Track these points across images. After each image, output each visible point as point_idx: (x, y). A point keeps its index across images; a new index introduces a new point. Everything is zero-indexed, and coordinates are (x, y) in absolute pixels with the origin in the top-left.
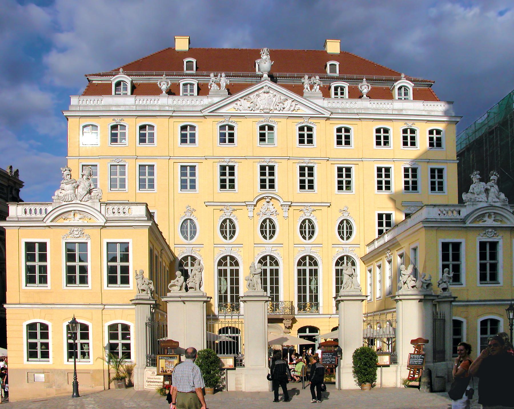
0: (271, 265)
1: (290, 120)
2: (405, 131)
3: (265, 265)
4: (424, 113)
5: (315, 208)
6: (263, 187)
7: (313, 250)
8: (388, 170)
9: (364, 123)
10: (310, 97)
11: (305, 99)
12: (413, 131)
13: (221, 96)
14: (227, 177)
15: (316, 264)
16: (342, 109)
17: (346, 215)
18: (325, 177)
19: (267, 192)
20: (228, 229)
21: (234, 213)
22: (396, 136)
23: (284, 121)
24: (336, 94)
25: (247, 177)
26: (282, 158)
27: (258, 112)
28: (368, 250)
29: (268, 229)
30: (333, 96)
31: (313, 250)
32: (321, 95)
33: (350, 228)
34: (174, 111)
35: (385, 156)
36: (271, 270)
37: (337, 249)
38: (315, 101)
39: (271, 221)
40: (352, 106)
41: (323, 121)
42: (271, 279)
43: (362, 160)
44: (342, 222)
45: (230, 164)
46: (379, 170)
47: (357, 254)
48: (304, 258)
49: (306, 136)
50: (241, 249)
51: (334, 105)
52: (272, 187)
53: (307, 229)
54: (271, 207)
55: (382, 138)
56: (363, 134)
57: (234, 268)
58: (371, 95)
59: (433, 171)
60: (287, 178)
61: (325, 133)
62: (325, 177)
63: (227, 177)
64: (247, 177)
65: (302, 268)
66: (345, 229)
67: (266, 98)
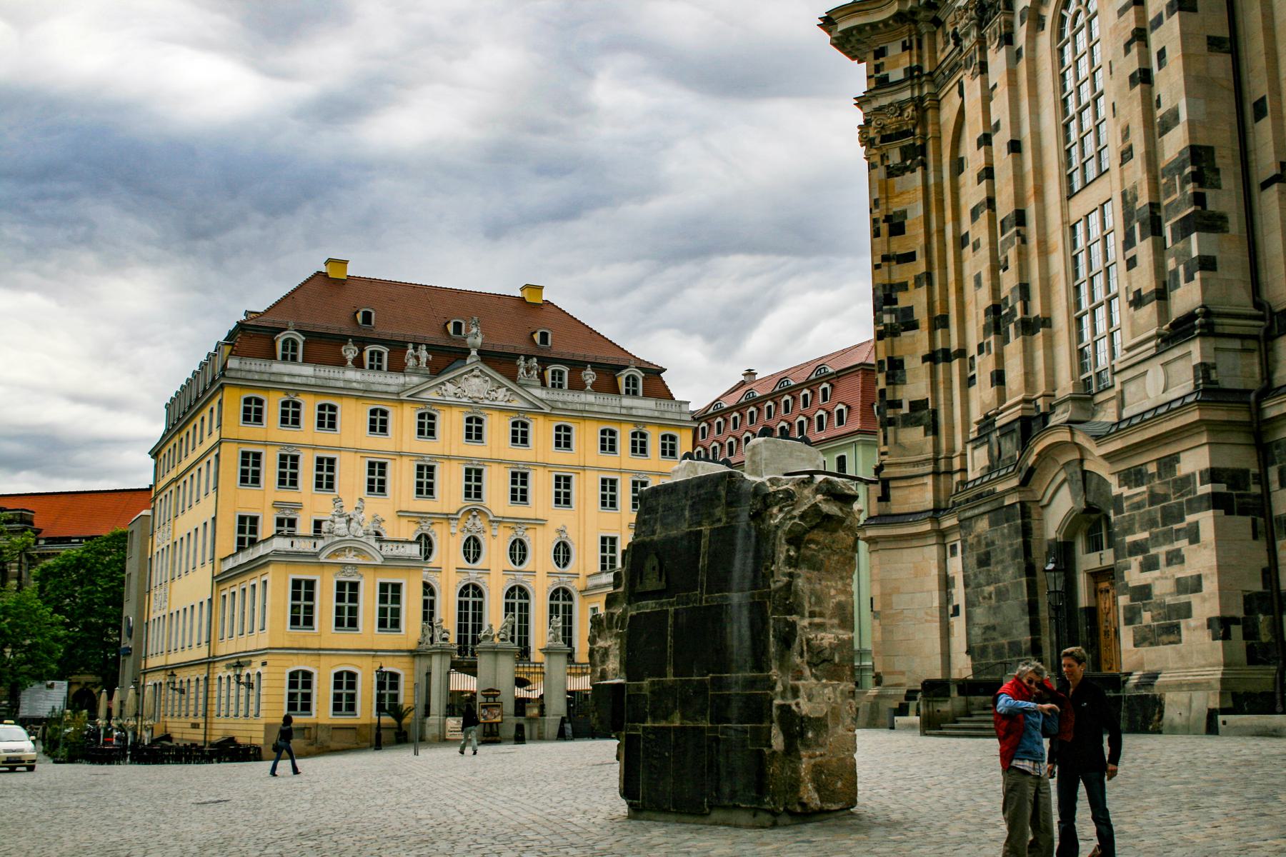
0: (474, 596)
2: (634, 435)
3: (467, 595)
4: (656, 414)
6: (468, 495)
7: (526, 579)
8: (613, 482)
9: (588, 423)
10: (527, 385)
11: (521, 386)
12: (643, 435)
13: (423, 375)
14: (425, 483)
15: (527, 597)
16: (564, 403)
17: (564, 535)
18: (541, 487)
19: (472, 503)
21: (433, 528)
23: (496, 414)
25: (450, 483)
26: (492, 461)
27: (465, 400)
28: (591, 582)
29: (473, 549)
31: (526, 579)
32: (539, 384)
33: (567, 551)
34: (366, 391)
36: (474, 603)
37: (551, 580)
39: (476, 540)
40: (576, 399)
41: (541, 419)
42: (474, 615)
43: (584, 468)
44: (558, 545)
46: (604, 481)
47: (575, 586)
48: (513, 589)
49: (520, 435)
51: (556, 397)
52: (478, 495)
53: (518, 551)
54: (478, 522)
55: (608, 444)
56: (586, 436)
57: (478, 599)
58: (597, 388)
60: (496, 486)
61: (542, 432)
62: (541, 487)
63: (425, 483)
64: (450, 483)
65: (510, 601)
66: (562, 553)
67: (475, 384)
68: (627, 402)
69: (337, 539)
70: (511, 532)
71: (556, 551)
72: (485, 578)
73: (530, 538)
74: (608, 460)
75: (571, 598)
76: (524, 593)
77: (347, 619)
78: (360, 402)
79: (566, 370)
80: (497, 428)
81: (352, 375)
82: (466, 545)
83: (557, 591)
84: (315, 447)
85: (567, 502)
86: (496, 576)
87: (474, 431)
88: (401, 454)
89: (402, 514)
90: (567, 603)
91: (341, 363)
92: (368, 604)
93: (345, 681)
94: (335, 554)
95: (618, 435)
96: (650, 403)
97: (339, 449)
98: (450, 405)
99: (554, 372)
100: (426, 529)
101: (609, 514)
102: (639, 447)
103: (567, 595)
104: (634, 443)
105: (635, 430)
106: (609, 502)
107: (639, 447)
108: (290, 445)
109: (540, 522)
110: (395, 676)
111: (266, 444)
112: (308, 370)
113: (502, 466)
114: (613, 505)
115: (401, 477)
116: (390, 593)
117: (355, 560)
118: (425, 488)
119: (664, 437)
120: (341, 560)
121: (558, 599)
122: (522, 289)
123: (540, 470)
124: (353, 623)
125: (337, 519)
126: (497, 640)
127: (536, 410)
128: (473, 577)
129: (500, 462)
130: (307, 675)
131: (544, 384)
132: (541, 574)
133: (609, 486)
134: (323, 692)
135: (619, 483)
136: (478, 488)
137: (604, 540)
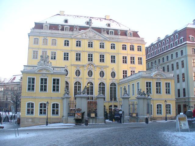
1: (97, 41)
2: (131, 46)
5: (104, 68)
6: (89, 60)
8: (126, 57)
12: (133, 46)
18: (108, 58)
19: (90, 62)
20: (78, 73)
22: (128, 47)
23: (96, 41)
24: (111, 33)
25: (84, 58)
26: (95, 52)
29: (90, 73)
30: (110, 34)
35: (124, 53)
38: (105, 35)
39: (91, 71)
44: (112, 72)
45: (79, 53)
47: (116, 82)
48: (101, 83)
50: (81, 80)
52: (92, 60)
53: (102, 74)
55: (124, 48)
59: (139, 58)
61: (108, 45)
62: (108, 58)
64: (84, 58)
66: (113, 75)
68: (129, 38)
69: (41, 66)
70: (100, 69)
71: (112, 74)
72: (93, 80)
73: (104, 71)
74: (124, 51)
75: (115, 85)
76: (104, 84)
77: (44, 88)
78: (62, 39)
79: (113, 31)
80: (96, 44)
81: (60, 32)
82: (89, 73)
83: (112, 84)
84: (51, 49)
85: (114, 62)
86: (96, 80)
87: (90, 45)
88: (72, 51)
89: (72, 65)
90: (115, 87)
91: (58, 30)
92: (50, 85)
93: (43, 106)
94: (40, 70)
95: (127, 46)
96: (135, 38)
97: (57, 50)
98: (84, 39)
99: (110, 32)
100: (78, 69)
101: (125, 64)
102: (132, 48)
103: (115, 85)
104: (131, 48)
105: (131, 45)
106: (125, 61)
107: (132, 48)
108: (45, 49)
109: (107, 67)
110: (57, 105)
111: (39, 49)
112: (50, 31)
113: (98, 53)
114: (126, 63)
115: (72, 57)
116: (56, 82)
117: (45, 72)
118: (78, 58)
119: (138, 47)
120: (41, 72)
121: (112, 86)
122: (105, 17)
123: (107, 54)
124: (45, 90)
125: (41, 61)
126: (82, 94)
127: (106, 39)
128: (91, 80)
129: (97, 52)
130: (32, 104)
131: (108, 33)
132: (108, 79)
133: (125, 58)
134: (37, 109)
135: (127, 57)
136: (92, 59)
137: (124, 71)
